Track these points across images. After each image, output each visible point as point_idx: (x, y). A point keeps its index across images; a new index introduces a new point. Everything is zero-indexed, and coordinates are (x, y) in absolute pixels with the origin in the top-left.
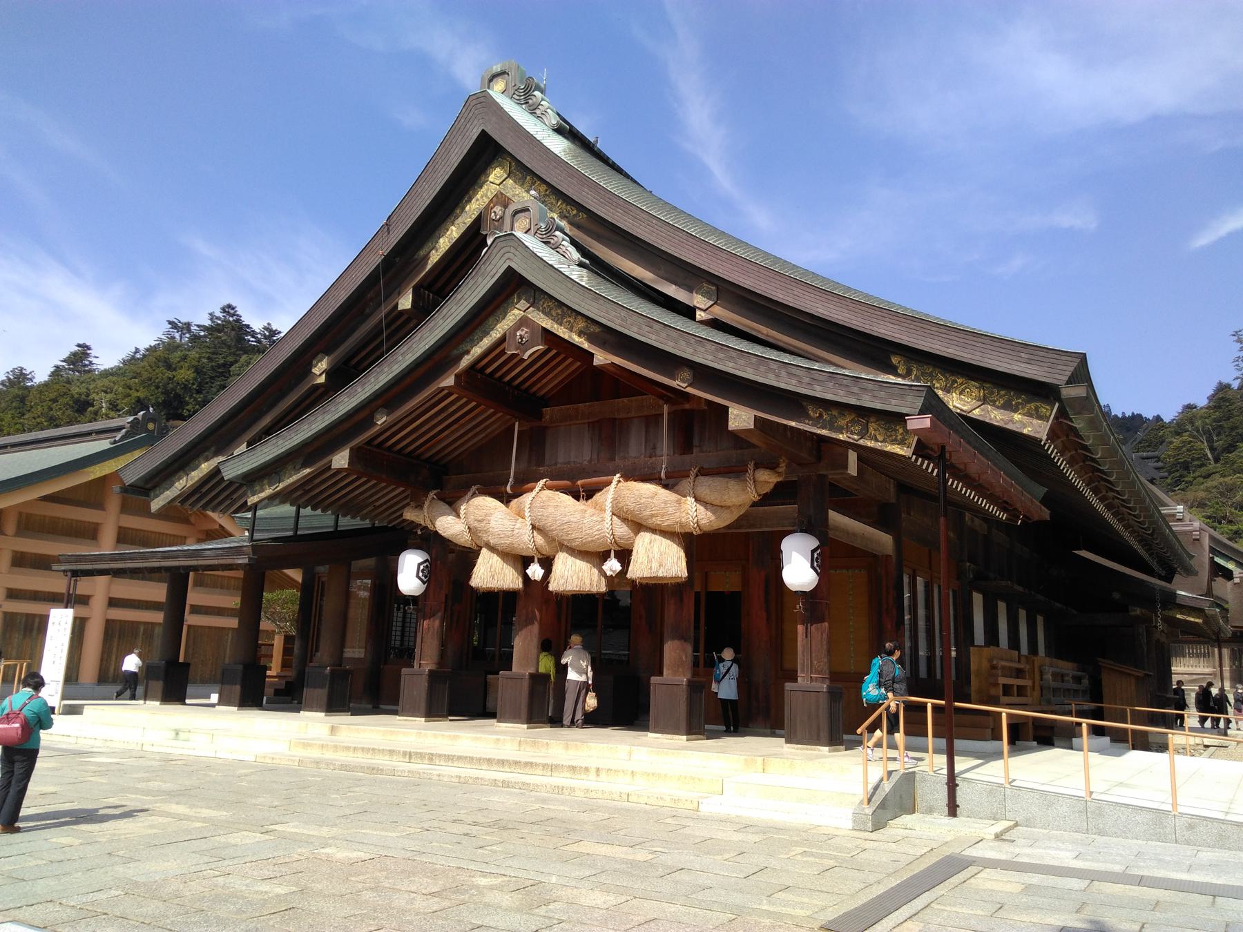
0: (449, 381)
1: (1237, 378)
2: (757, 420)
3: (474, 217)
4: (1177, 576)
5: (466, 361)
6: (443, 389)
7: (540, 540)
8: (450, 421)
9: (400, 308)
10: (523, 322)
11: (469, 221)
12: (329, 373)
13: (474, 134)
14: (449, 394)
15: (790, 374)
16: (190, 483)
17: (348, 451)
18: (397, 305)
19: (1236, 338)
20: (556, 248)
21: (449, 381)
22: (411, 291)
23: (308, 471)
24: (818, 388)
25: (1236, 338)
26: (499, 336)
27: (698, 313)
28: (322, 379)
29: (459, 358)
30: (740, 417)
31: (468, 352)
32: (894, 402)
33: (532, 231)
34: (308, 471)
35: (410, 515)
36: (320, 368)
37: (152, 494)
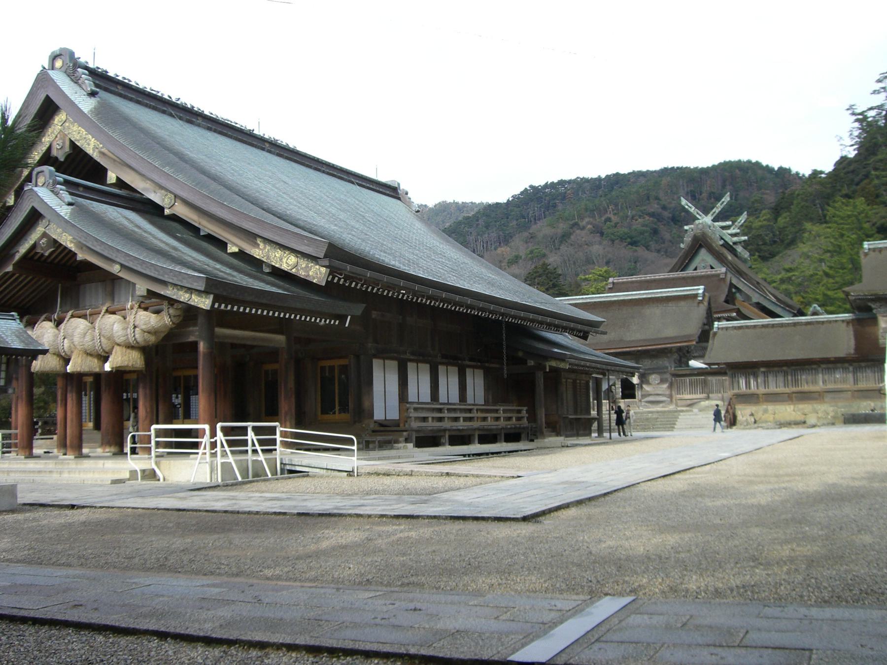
0: (10, 268)
1: (852, 145)
3: (47, 146)
4: (590, 336)
5: (17, 257)
6: (8, 273)
8: (21, 285)
9: (8, 204)
11: (44, 149)
13: (42, 97)
14: (13, 275)
15: (156, 270)
18: (5, 203)
19: (850, 112)
20: (56, 194)
21: (10, 268)
22: (13, 193)
24: (166, 276)
25: (850, 112)
26: (33, 242)
27: (166, 210)
29: (14, 255)
31: (18, 251)
32: (195, 284)
33: (46, 185)
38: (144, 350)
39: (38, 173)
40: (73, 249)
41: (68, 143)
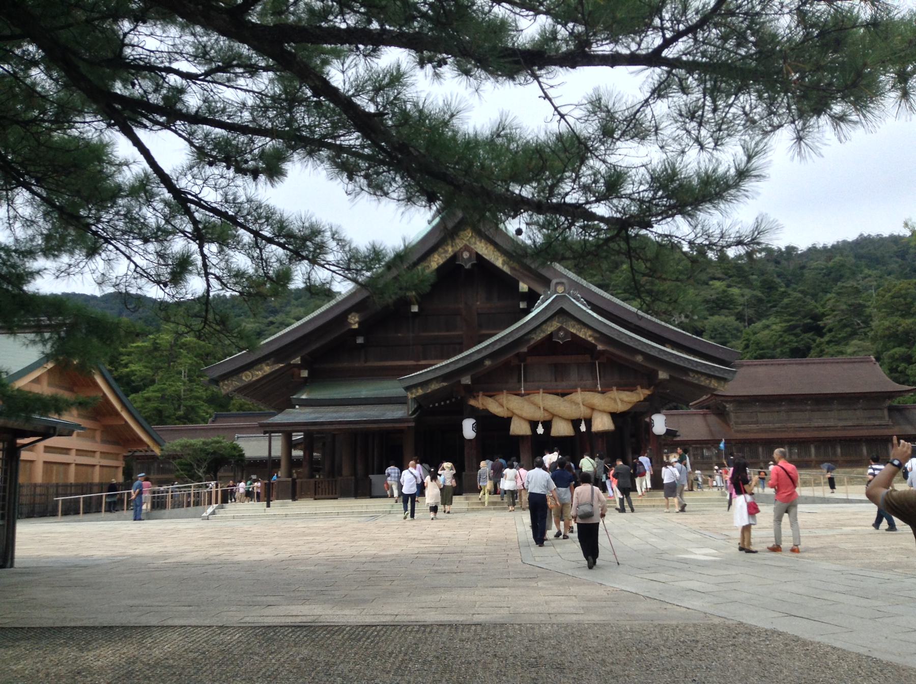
2: (670, 376)
3: (452, 254)
7: (546, 414)
10: (560, 329)
11: (448, 256)
12: (360, 323)
15: (689, 363)
16: (254, 379)
17: (469, 377)
23: (445, 384)
28: (356, 326)
30: (663, 375)
34: (445, 384)
35: (472, 402)
36: (354, 321)
37: (221, 384)
38: (614, 416)
39: (557, 284)
40: (593, 342)
41: (474, 256)
